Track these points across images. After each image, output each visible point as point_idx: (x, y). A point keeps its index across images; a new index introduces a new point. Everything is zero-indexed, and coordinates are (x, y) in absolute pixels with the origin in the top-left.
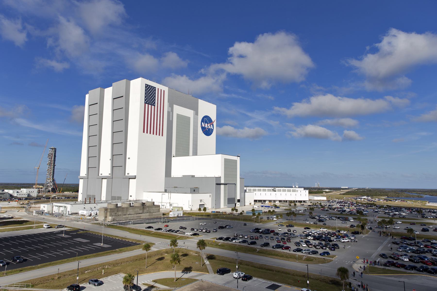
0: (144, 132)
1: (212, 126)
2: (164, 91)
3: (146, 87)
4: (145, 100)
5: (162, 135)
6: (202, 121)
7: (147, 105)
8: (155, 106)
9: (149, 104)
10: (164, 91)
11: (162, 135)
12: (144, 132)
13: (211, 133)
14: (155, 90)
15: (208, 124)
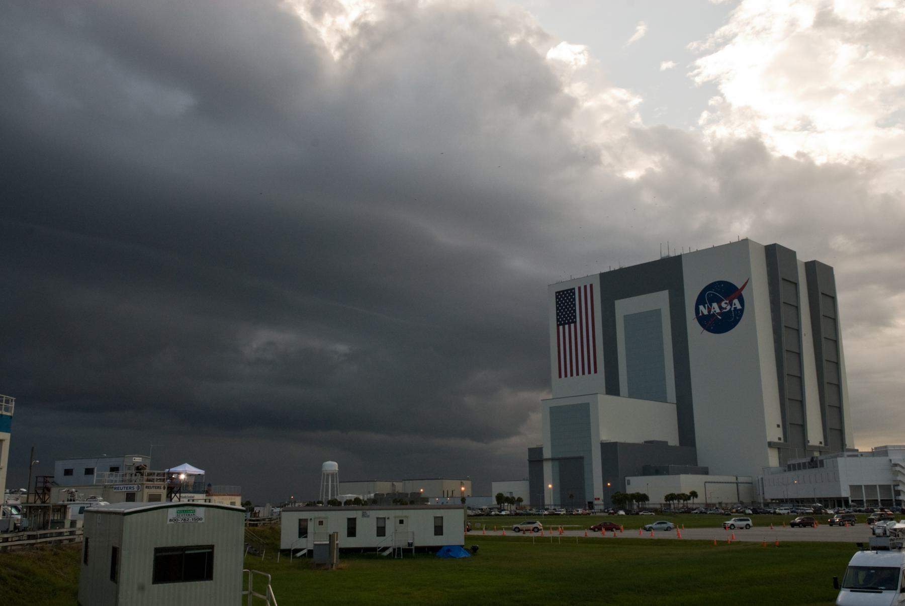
0: (560, 377)
1: (736, 301)
2: (591, 286)
3: (557, 297)
4: (558, 320)
5: (596, 372)
6: (701, 300)
7: (561, 327)
8: (575, 323)
9: (564, 325)
10: (591, 286)
11: (596, 372)
12: (560, 377)
13: (736, 322)
14: (574, 294)
15: (719, 302)
